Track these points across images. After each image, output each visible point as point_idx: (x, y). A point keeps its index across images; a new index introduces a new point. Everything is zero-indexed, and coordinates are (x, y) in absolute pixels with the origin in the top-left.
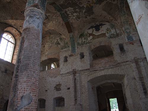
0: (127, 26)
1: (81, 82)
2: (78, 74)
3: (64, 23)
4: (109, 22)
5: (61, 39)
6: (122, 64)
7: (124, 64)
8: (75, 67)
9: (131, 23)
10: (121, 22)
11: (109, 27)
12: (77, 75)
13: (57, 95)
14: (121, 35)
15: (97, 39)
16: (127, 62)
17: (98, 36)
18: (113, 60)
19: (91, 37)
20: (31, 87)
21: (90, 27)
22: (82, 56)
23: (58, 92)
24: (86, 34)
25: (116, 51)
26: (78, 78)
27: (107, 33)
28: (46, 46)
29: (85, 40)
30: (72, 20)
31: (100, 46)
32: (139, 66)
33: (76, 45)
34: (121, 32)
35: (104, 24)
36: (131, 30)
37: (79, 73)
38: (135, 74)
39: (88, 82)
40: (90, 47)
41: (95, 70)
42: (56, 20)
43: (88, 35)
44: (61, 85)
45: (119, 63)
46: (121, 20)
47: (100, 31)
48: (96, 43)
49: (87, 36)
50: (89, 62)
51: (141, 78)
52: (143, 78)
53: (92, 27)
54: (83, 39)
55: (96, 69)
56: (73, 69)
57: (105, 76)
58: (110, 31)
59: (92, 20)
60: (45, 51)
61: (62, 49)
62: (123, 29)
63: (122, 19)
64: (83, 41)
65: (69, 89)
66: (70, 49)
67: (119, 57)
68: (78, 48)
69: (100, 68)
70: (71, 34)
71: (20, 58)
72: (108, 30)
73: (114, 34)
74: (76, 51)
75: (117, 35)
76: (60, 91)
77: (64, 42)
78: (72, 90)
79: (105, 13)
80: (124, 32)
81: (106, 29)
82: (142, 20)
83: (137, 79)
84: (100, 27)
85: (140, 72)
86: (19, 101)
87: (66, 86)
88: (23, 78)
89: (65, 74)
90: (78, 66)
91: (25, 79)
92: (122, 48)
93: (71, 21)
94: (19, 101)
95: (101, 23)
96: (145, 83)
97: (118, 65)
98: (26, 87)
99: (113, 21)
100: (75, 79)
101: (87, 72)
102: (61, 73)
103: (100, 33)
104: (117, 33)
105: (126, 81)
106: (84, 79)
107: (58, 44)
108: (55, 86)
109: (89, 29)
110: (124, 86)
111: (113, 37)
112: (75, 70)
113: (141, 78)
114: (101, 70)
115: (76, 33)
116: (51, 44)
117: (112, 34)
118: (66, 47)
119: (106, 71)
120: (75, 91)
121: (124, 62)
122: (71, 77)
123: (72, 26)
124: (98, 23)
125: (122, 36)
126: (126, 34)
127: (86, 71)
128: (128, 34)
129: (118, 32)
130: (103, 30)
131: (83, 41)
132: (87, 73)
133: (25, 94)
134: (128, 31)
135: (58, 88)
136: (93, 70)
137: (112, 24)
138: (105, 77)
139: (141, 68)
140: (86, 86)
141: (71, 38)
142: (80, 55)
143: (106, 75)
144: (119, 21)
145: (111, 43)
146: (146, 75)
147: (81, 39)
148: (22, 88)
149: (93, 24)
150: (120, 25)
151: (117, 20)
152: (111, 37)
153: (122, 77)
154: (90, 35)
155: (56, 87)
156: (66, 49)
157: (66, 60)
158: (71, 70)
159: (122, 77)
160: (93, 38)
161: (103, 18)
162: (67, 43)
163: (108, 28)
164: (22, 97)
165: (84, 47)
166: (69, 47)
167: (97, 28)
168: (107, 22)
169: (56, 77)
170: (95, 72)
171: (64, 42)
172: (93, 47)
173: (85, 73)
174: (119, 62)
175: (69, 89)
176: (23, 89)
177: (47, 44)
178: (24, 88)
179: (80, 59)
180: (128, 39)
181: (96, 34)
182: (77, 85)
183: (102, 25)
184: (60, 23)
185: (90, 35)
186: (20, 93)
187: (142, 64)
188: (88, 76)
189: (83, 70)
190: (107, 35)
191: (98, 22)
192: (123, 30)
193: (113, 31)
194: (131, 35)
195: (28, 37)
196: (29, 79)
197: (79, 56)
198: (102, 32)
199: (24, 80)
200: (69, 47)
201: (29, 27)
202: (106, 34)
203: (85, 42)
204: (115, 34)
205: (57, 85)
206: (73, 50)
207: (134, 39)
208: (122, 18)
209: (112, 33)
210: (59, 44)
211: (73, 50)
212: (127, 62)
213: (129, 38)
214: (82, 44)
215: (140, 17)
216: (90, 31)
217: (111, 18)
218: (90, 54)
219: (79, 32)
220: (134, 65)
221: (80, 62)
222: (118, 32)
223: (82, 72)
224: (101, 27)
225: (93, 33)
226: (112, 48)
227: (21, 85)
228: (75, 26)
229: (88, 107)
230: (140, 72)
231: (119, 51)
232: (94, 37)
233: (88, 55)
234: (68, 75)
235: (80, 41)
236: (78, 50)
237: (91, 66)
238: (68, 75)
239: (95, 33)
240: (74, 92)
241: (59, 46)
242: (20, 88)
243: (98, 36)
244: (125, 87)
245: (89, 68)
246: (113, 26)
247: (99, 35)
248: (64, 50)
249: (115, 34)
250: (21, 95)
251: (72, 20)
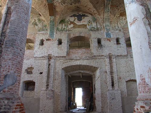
0: (108, 24)
1: (55, 68)
2: (53, 60)
3: (47, 4)
4: (92, 15)
5: (39, 20)
6: (97, 57)
7: (100, 57)
8: (50, 52)
9: (112, 22)
10: (104, 18)
11: (91, 20)
12: (52, 60)
14: (101, 30)
15: (77, 29)
16: (102, 56)
17: (80, 26)
18: (90, 52)
19: (72, 25)
20: (16, 66)
21: (72, 15)
22: (60, 42)
23: (29, 75)
24: (67, 21)
25: (94, 44)
26: (52, 64)
27: (89, 25)
29: (65, 27)
30: (57, 3)
31: (79, 36)
32: (112, 62)
33: (55, 30)
34: (101, 28)
35: (87, 16)
36: (111, 28)
37: (55, 59)
38: (108, 69)
39: (63, 69)
40: (69, 35)
41: (71, 58)
43: (69, 22)
44: (33, 68)
45: (95, 56)
46: (104, 16)
47: (82, 21)
48: (77, 32)
49: (68, 23)
50: (66, 50)
51: (112, 73)
52: (113, 72)
53: (74, 16)
54: (63, 25)
55: (73, 58)
56: (48, 53)
57: (80, 66)
58: (92, 24)
59: (76, 8)
61: (39, 31)
62: (104, 25)
63: (105, 16)
64: (64, 27)
65: (41, 73)
66: (49, 32)
67: (96, 51)
68: (56, 33)
69: (76, 57)
70: (52, 18)
71: (4, 31)
72: (89, 22)
73: (94, 28)
74: (55, 36)
75: (98, 29)
76: (32, 75)
77: (43, 24)
78: (45, 75)
79: (90, 5)
80: (104, 27)
81: (88, 21)
82: (136, 22)
83: (109, 73)
84: (83, 17)
85: (111, 67)
86: (2, 80)
87: (39, 70)
88: (8, 55)
89: (39, 58)
90: (55, 51)
91: (10, 56)
92: (99, 42)
93: (55, 4)
94: (2, 80)
95: (84, 14)
96: (113, 77)
97: (93, 57)
98: (11, 66)
99: (97, 15)
100: (50, 65)
101: (62, 59)
102: (35, 56)
103: (81, 24)
104: (97, 27)
105: (98, 73)
106: (59, 66)
108: (26, 68)
109: (71, 16)
110: (95, 77)
111: (92, 30)
112: (50, 56)
113: (112, 73)
114: (77, 60)
115: (58, 18)
117: (92, 27)
118: (43, 30)
119: (81, 61)
120: (48, 77)
121: (100, 56)
122: (46, 62)
123: (54, 9)
124: (81, 13)
125: (102, 31)
126: (105, 30)
127: (62, 58)
128: (108, 30)
129: (98, 27)
130: (85, 21)
131: (64, 27)
132: (63, 60)
133: (9, 73)
134: (108, 28)
135: (29, 71)
136: (69, 58)
137: (94, 18)
138: (80, 67)
139: (113, 64)
140: (60, 73)
141: (51, 21)
142: (58, 41)
143: (81, 65)
144: (102, 16)
145: (90, 35)
146: (116, 71)
147: (61, 25)
148: (6, 66)
149: (76, 13)
150: (102, 21)
151: (100, 15)
152: (91, 30)
153: (95, 69)
154: (72, 23)
155: (26, 69)
156: (43, 32)
157: (42, 43)
158: (46, 55)
159: (95, 69)
160: (74, 27)
161: (87, 9)
162: (45, 26)
163: (90, 21)
164: (6, 76)
165: (63, 34)
166: (47, 30)
167: (80, 18)
168: (90, 14)
170: (71, 60)
171: (43, 24)
172: (72, 36)
173: (60, 60)
174: (95, 55)
175: (41, 73)
176: (7, 67)
178: (9, 66)
179: (57, 45)
180: (107, 36)
181: (77, 24)
182: (51, 71)
183: (84, 16)
185: (72, 23)
186: (3, 71)
187: (114, 60)
188: (64, 63)
189: (59, 56)
190: (88, 27)
191: (81, 12)
192: (103, 26)
193: (94, 25)
194: (110, 32)
195: (17, 9)
196: (15, 56)
197: (57, 42)
198: (84, 23)
199: (9, 57)
200: (47, 30)
202: (87, 26)
203: (64, 28)
204: (96, 27)
205: (29, 68)
206: (52, 34)
207: (112, 37)
208: (105, 14)
209: (93, 26)
210: (37, 25)
211: (52, 34)
212: (102, 56)
213: (108, 35)
214: (62, 30)
215: (135, 19)
216: (72, 19)
217: (95, 12)
218: (68, 41)
219: (60, 17)
220: (107, 60)
221: (57, 48)
222: (98, 27)
223: (57, 58)
224: (84, 18)
225: (75, 22)
226: (90, 40)
227: (5, 63)
228: (58, 9)
229: (59, 93)
230: (111, 67)
231: (96, 44)
232: (75, 26)
233: (66, 42)
234: (42, 59)
235: (60, 27)
236: (57, 36)
237: (68, 54)
238: (42, 59)
239: (76, 22)
240: (46, 78)
241: (36, 27)
242: (4, 65)
243: (80, 26)
244: (96, 79)
245: (65, 55)
246: (95, 20)
247: (80, 25)
248: (41, 32)
249: (96, 27)
250: (5, 73)
251: (56, 3)
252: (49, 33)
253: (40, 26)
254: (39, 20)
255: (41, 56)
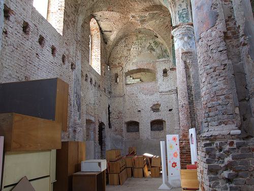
5: (156, 43)
13: (155, 116)
23: (157, 113)
28: (132, 49)
42: (162, 20)
44: (160, 105)
60: (132, 57)
61: (159, 58)
65: (170, 110)
76: (160, 113)
87: (167, 107)
89: (167, 92)
102: (160, 90)
107: (152, 49)
116: (140, 49)
118: (164, 57)
135: (156, 108)
156: (164, 59)
157: (165, 72)
166: (168, 56)
169: (152, 94)
175: (170, 110)
177: (133, 46)
184: (164, 23)
201: (190, 51)
205: (154, 105)
241: (154, 53)
248: (161, 60)
252: (172, 61)
253: (158, 51)
254: (156, 43)
255: (167, 90)
